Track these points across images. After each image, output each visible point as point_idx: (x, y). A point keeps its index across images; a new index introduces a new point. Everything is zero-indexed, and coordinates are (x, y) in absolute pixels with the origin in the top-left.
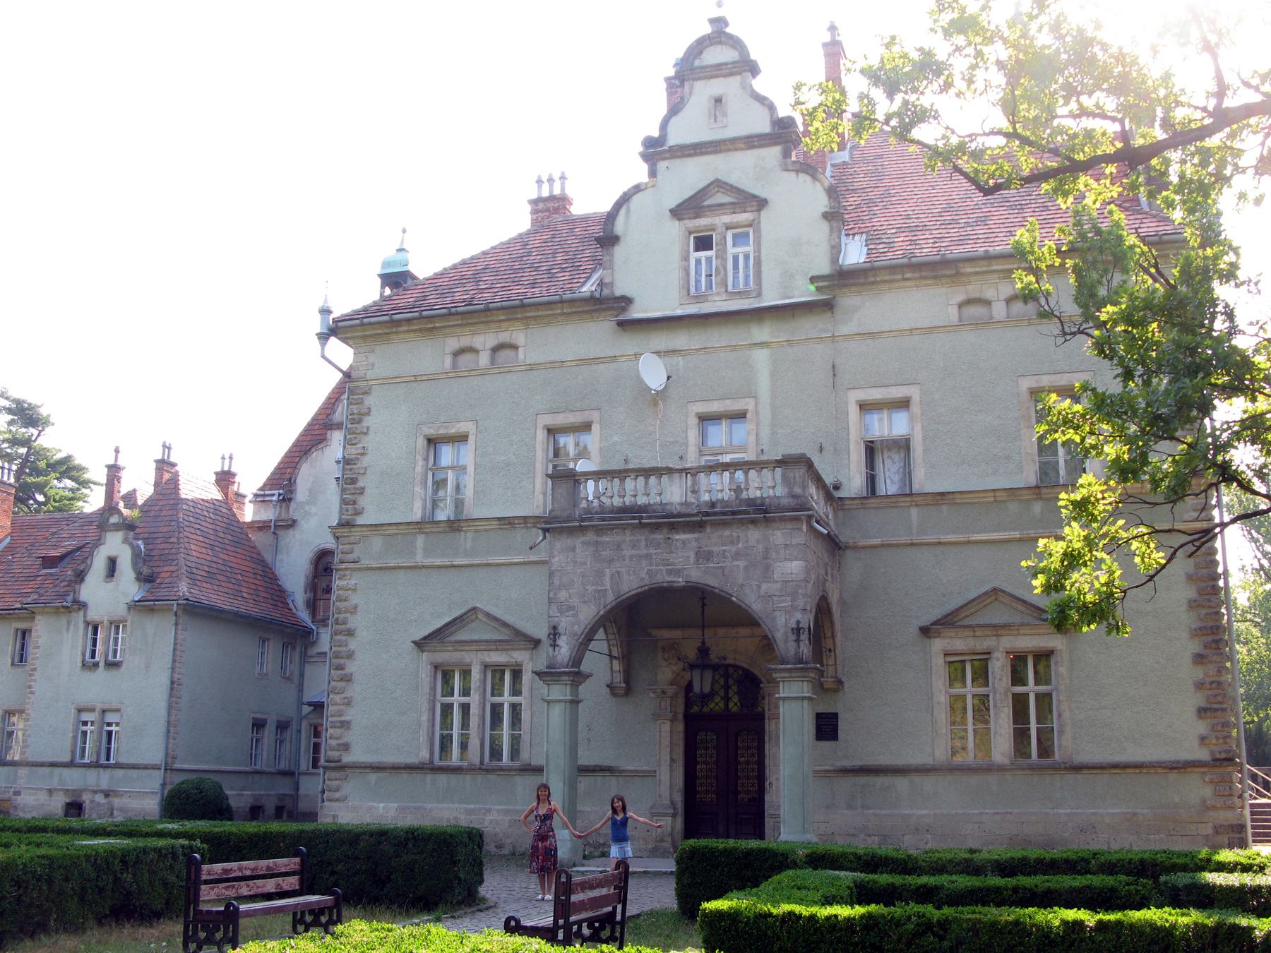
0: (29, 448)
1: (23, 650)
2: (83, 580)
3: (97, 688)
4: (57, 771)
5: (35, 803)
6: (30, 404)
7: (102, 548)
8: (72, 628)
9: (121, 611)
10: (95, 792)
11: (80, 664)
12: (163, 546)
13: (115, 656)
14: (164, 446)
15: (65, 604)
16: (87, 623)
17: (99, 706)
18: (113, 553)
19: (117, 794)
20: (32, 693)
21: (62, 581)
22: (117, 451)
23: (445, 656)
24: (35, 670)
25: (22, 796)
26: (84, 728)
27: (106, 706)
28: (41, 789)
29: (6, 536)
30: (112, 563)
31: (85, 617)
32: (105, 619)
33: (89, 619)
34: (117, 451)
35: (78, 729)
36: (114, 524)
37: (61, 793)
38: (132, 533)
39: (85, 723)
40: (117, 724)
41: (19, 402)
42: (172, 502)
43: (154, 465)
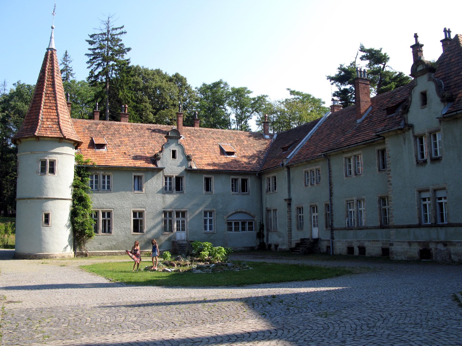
0: (381, 74)
1: (384, 162)
2: (408, 111)
4: (412, 230)
6: (375, 51)
7: (416, 88)
8: (407, 141)
9: (435, 124)
10: (437, 243)
11: (415, 163)
12: (456, 79)
13: (436, 154)
14: (445, 31)
15: (400, 127)
16: (415, 137)
17: (431, 187)
18: (423, 90)
19: (452, 244)
20: (391, 184)
21: (396, 116)
22: (416, 36)
24: (390, 170)
25: (394, 246)
26: (424, 203)
27: (436, 187)
28: (404, 242)
29: (369, 107)
30: (424, 95)
31: (413, 133)
32: (426, 131)
33: (416, 134)
34: (416, 36)
35: (420, 203)
36: (421, 71)
37: (416, 244)
38: (433, 74)
39: (424, 199)
40: (445, 198)
41: (370, 51)
42: (456, 53)
43: (441, 44)
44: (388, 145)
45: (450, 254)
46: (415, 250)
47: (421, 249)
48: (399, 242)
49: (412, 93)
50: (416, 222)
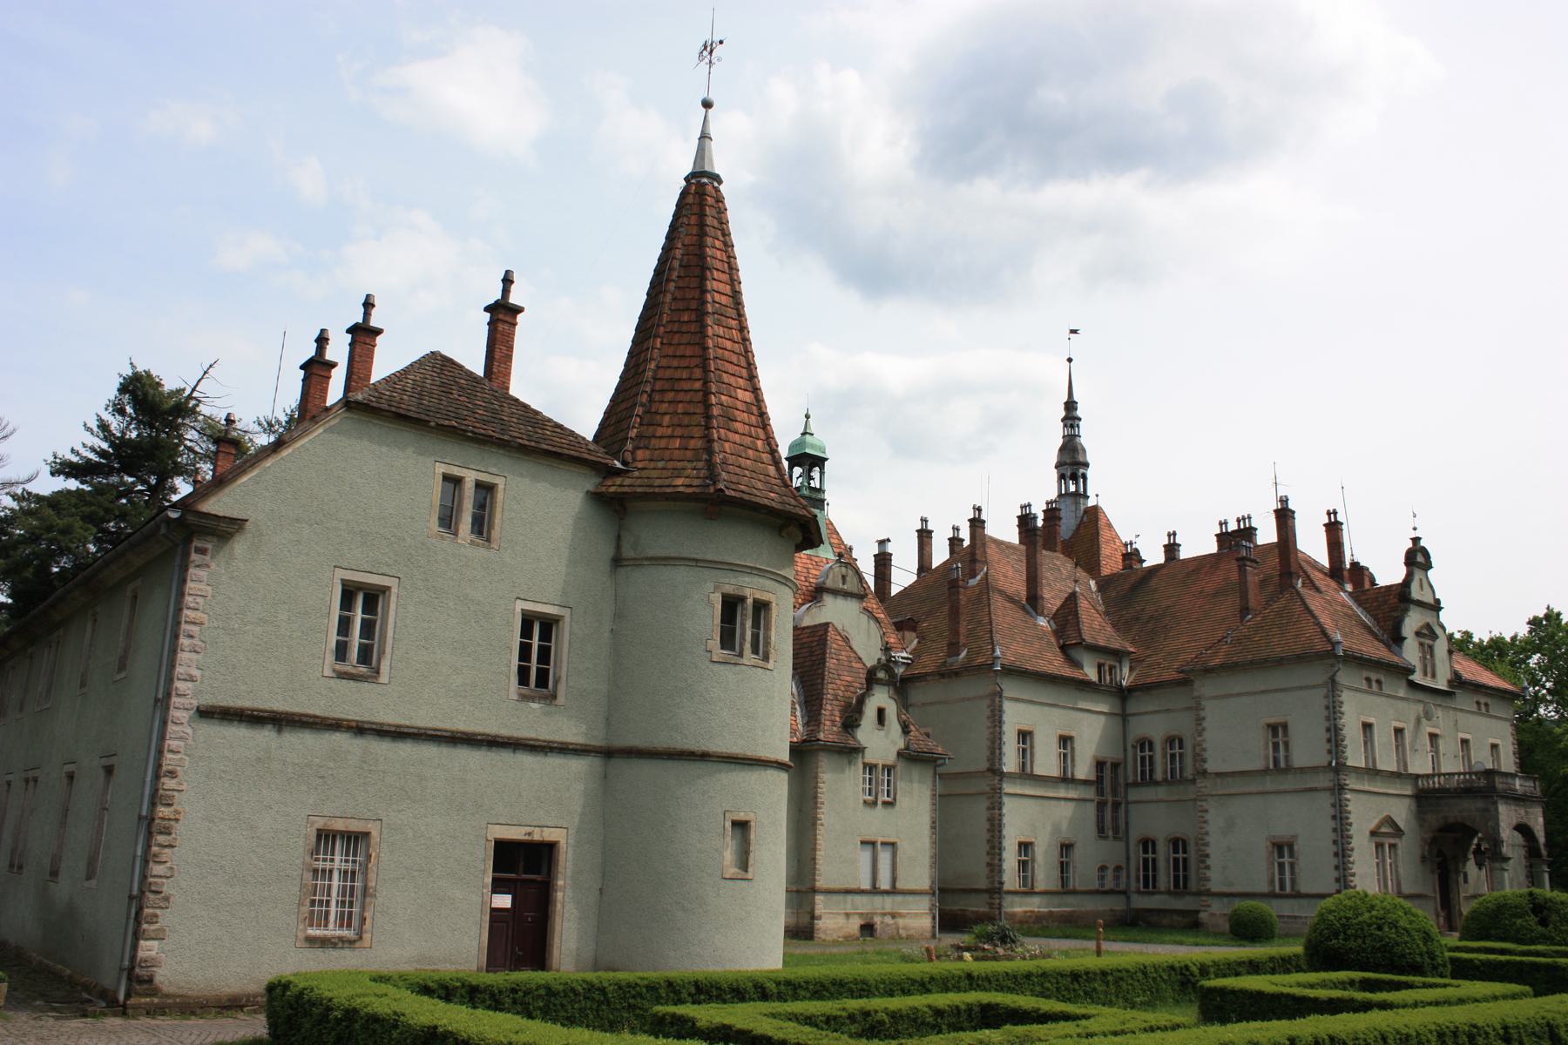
3: (878, 824)
4: (849, 898)
5: (835, 926)
7: (872, 698)
9: (891, 758)
11: (861, 802)
16: (865, 765)
17: (880, 840)
18: (882, 705)
19: (901, 915)
20: (822, 825)
23: (1378, 839)
25: (823, 920)
30: (881, 713)
33: (866, 760)
37: (856, 916)
44: (823, 764)
45: (898, 929)
46: (854, 925)
47: (862, 923)
48: (832, 913)
49: (867, 701)
50: (866, 885)
